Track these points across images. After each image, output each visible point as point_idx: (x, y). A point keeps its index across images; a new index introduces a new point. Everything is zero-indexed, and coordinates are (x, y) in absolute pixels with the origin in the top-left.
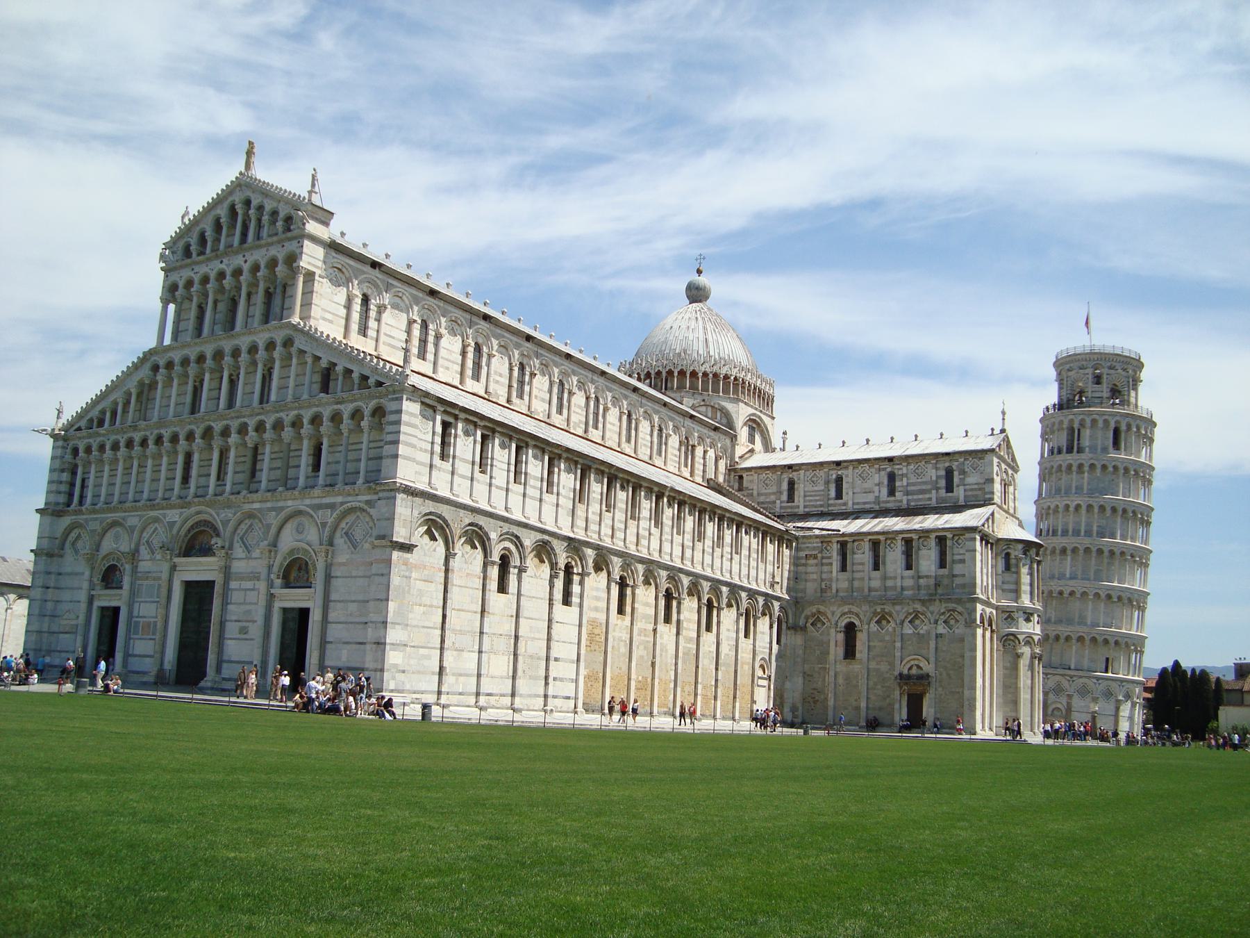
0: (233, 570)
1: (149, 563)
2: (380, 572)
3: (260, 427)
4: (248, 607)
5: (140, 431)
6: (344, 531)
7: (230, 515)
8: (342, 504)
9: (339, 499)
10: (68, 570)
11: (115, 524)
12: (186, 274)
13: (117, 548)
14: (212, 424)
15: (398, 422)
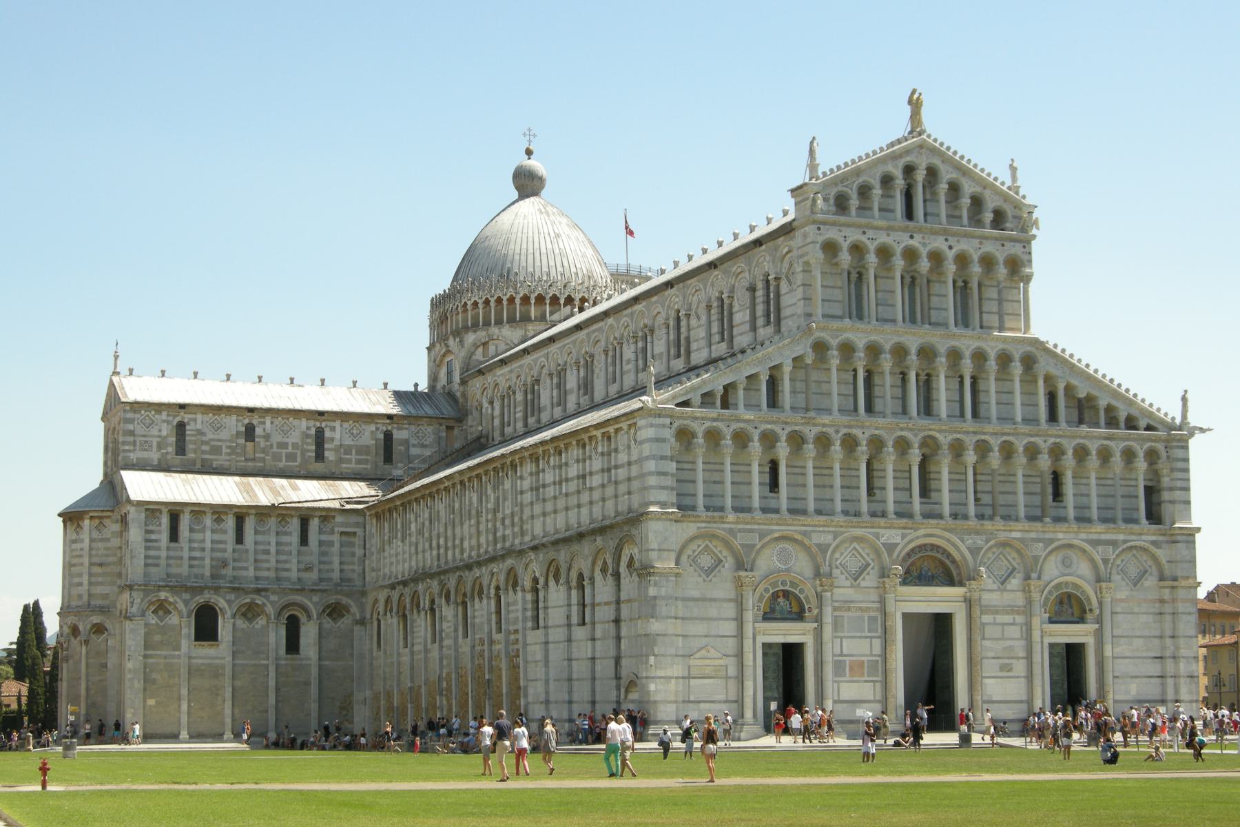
0: (984, 603)
1: (851, 591)
2: (1187, 611)
3: (1008, 452)
4: (1008, 643)
5: (815, 425)
6: (1120, 568)
7: (980, 542)
8: (1125, 542)
9: (1121, 537)
10: (695, 593)
11: (784, 538)
12: (854, 236)
13: (787, 570)
14: (937, 435)
15: (1187, 470)
